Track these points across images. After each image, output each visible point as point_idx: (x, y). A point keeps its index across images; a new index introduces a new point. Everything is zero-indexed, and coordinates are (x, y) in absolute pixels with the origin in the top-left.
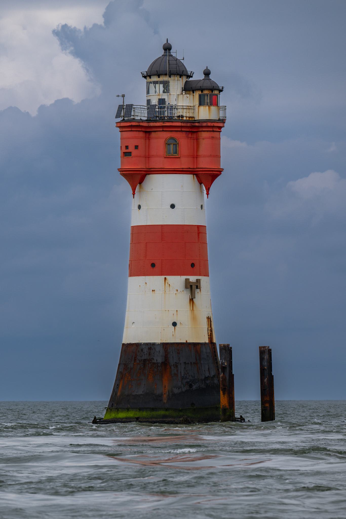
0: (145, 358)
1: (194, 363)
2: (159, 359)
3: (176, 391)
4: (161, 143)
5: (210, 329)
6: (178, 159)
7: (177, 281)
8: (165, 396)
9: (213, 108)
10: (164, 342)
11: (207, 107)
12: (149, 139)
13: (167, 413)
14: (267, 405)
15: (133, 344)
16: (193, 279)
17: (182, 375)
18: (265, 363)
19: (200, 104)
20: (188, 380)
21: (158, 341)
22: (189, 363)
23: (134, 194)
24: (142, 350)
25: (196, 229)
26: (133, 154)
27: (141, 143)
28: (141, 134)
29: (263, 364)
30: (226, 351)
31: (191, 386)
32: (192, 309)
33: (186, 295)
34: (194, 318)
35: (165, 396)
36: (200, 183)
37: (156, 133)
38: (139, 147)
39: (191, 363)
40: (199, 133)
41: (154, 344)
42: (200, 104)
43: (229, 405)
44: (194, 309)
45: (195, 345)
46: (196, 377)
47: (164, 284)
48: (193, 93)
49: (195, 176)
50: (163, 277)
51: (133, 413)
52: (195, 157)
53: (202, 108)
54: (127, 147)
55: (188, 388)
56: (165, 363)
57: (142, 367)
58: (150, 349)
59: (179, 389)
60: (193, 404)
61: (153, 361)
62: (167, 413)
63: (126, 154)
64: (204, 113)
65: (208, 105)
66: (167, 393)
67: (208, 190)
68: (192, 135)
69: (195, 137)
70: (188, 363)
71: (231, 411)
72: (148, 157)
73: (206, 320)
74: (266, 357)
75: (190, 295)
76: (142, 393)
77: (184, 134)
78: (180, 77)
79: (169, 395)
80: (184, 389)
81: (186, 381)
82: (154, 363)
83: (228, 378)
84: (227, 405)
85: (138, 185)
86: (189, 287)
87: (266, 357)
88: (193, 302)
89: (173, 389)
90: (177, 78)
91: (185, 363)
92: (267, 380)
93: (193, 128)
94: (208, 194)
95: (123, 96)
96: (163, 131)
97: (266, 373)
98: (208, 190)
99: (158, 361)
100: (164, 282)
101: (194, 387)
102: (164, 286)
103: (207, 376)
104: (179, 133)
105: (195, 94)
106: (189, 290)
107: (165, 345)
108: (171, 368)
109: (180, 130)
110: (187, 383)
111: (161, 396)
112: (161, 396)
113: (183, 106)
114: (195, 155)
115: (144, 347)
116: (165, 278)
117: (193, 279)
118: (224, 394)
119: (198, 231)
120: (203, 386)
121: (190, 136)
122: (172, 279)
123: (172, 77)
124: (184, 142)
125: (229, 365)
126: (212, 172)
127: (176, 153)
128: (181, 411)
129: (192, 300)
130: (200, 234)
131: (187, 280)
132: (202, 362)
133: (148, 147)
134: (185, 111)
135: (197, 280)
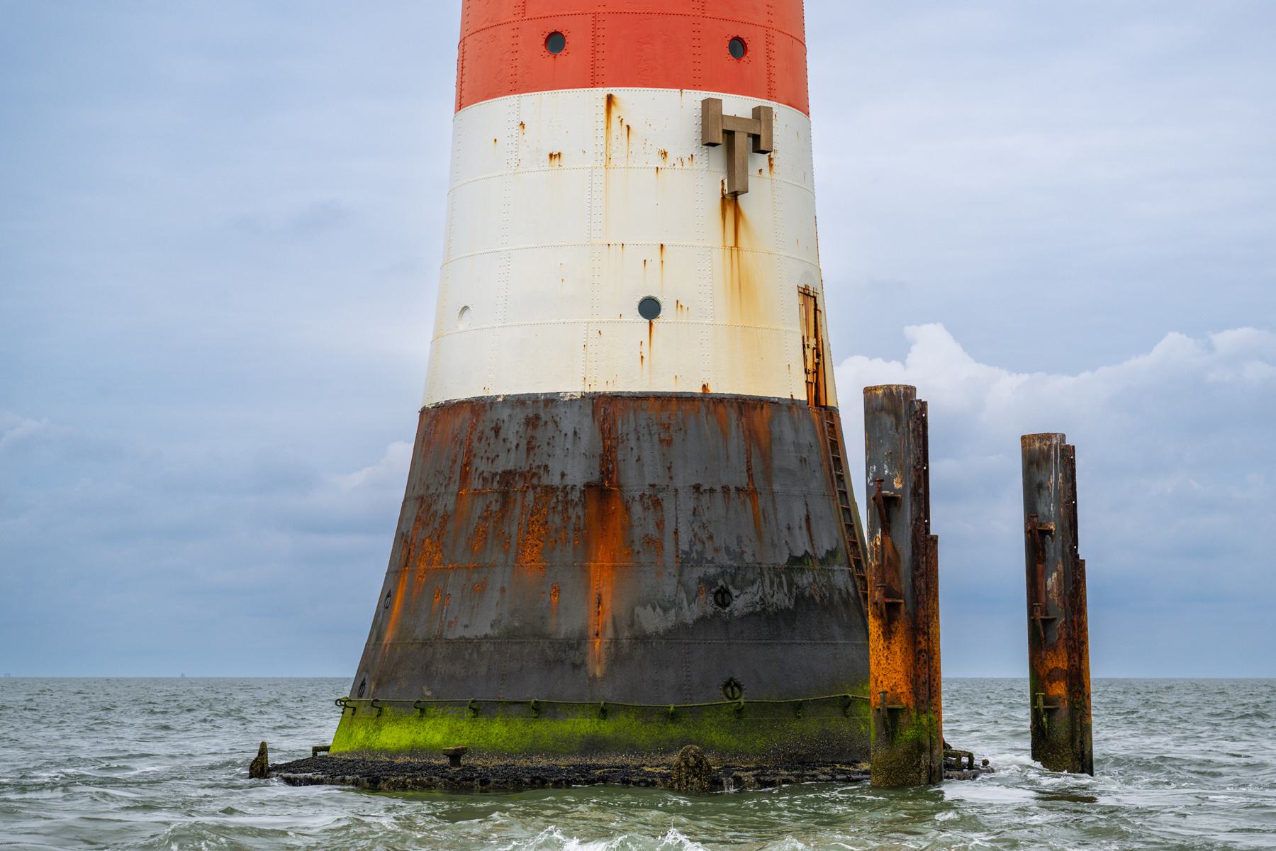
0: (510, 467)
1: (738, 489)
2: (572, 467)
3: (653, 621)
5: (812, 342)
8: (598, 647)
10: (602, 388)
13: (606, 728)
14: (1059, 689)
15: (460, 405)
16: (737, 106)
17: (684, 546)
18: (1049, 509)
20: (712, 571)
21: (571, 385)
22: (718, 488)
24: (497, 430)
30: (898, 418)
31: (723, 598)
32: (731, 242)
33: (707, 178)
34: (741, 286)
35: (598, 647)
39: (726, 490)
41: (551, 400)
43: (915, 692)
44: (743, 242)
45: (746, 405)
46: (748, 558)
47: (603, 126)
50: (601, 93)
51: (445, 729)
55: (710, 610)
56: (603, 490)
57: (495, 507)
58: (532, 422)
59: (665, 610)
60: (732, 685)
61: (545, 480)
62: (606, 728)
66: (609, 633)
70: (712, 490)
71: (924, 721)
73: (797, 300)
74: (1053, 479)
76: (488, 631)
79: (616, 641)
80: (691, 613)
81: (698, 572)
82: (549, 490)
83: (906, 552)
84: (903, 688)
86: (719, 138)
87: (1053, 479)
88: (737, 214)
89: (638, 610)
91: (697, 488)
92: (1058, 579)
97: (1053, 548)
99: (569, 481)
100: (603, 117)
102: (602, 133)
103: (799, 553)
106: (718, 154)
107: (606, 408)
108: (628, 510)
110: (707, 582)
111: (578, 643)
112: (578, 643)
115: (505, 414)
116: (610, 99)
117: (737, 106)
118: (888, 634)
120: (781, 599)
125: (915, 493)
128: (673, 717)
129: (731, 200)
132: (777, 487)
135: (757, 111)
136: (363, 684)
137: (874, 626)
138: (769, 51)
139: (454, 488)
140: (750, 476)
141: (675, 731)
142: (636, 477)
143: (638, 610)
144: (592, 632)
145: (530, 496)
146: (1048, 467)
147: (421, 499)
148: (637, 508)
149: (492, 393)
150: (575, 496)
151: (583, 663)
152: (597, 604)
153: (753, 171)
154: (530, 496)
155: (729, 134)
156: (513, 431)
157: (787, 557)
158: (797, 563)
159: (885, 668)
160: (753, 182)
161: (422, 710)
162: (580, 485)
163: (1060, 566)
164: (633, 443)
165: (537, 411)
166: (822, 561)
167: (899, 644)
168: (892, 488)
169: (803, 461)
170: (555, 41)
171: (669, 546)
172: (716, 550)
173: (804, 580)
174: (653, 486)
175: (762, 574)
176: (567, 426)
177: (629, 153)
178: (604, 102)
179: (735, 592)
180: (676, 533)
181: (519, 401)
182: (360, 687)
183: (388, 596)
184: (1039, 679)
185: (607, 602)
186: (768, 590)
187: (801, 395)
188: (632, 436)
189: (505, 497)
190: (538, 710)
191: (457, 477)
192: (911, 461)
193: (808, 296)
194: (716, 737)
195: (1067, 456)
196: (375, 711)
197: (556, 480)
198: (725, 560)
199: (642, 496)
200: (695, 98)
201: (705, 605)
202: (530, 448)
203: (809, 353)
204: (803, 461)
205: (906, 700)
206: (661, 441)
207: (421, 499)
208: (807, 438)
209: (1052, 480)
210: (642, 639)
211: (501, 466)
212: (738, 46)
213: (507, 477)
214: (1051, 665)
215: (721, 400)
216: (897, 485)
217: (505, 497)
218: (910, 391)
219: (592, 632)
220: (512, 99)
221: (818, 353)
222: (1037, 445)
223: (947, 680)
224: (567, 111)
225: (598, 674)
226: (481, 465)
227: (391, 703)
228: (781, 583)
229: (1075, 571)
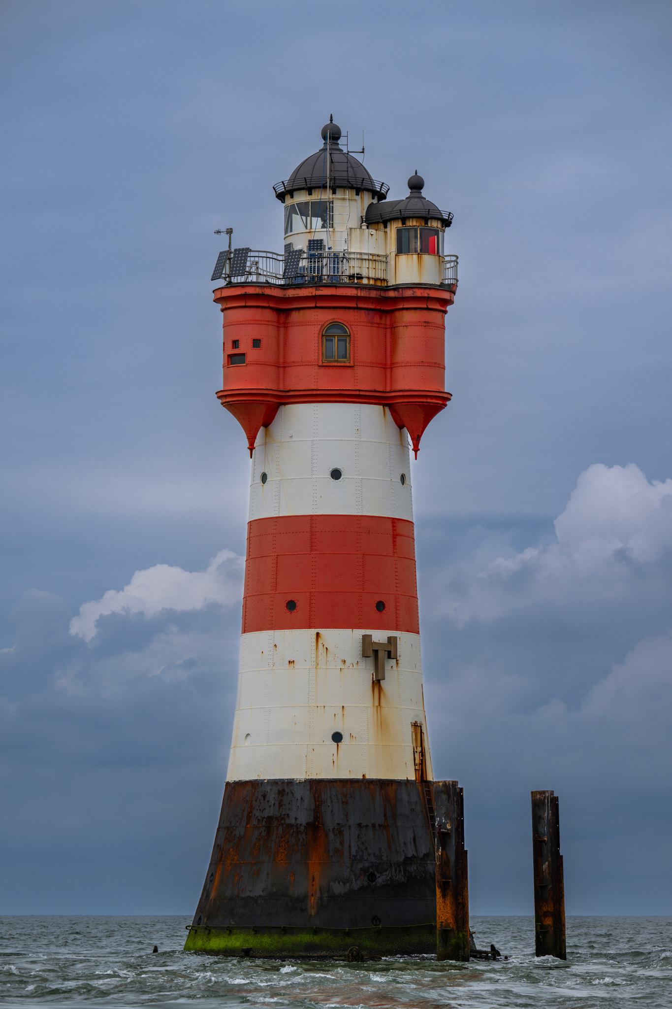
0: (271, 814)
1: (379, 825)
2: (301, 816)
3: (338, 889)
4: (313, 332)
5: (419, 749)
6: (349, 370)
7: (345, 641)
8: (313, 901)
9: (427, 259)
10: (314, 777)
11: (415, 257)
12: (286, 326)
13: (317, 939)
14: (549, 921)
15: (247, 782)
16: (379, 636)
17: (353, 853)
18: (545, 829)
19: (400, 251)
20: (367, 865)
21: (300, 775)
22: (370, 825)
23: (251, 448)
24: (264, 796)
25: (389, 525)
26: (249, 358)
27: (267, 333)
28: (268, 315)
29: (541, 829)
30: (449, 796)
31: (372, 877)
32: (377, 704)
33: (364, 674)
34: (382, 725)
35: (313, 901)
36: (401, 427)
37: (301, 312)
38: (264, 344)
39: (374, 825)
40: (397, 313)
41: (290, 782)
42: (400, 251)
43: (457, 922)
44: (383, 704)
45: (384, 784)
46: (384, 858)
47: (314, 648)
48: (386, 227)
49: (387, 409)
50: (314, 631)
51: (241, 940)
52: (387, 366)
53: (403, 258)
54: (235, 344)
55: (366, 883)
56: (315, 826)
57: (264, 834)
58: (281, 793)
59: (344, 884)
60: (376, 919)
61: (288, 821)
62: (317, 939)
63: (234, 359)
64: (408, 271)
65: (416, 251)
66: (318, 894)
67: (416, 440)
68: (381, 318)
69: (388, 322)
70: (367, 826)
71: (461, 935)
72: (281, 366)
73: (410, 730)
74: (547, 814)
75: (373, 671)
76: (261, 893)
78: (357, 194)
79: (321, 899)
80: (356, 885)
81: (360, 866)
82: (290, 826)
83: (452, 858)
84: (451, 920)
86: (371, 653)
87: (547, 814)
88: (380, 690)
89: (332, 883)
90: (348, 194)
91: (360, 825)
92: (549, 866)
93: (384, 303)
94: (416, 449)
95: (230, 232)
96: (316, 307)
97: (546, 850)
98: (416, 440)
99: (299, 822)
100: (314, 644)
101: (380, 880)
102: (314, 652)
103: (410, 856)
104: (351, 312)
105: (388, 230)
106: (371, 661)
107: (315, 785)
108: (327, 836)
109: (353, 305)
110: (364, 870)
111: (303, 899)
112: (303, 899)
113: (361, 254)
114: (389, 362)
115: (268, 788)
116: (318, 634)
117: (379, 636)
118: (444, 896)
119: (394, 530)
120: (400, 878)
121: (377, 319)
122: (330, 635)
123: (339, 194)
124: (362, 332)
125: (457, 830)
126: (425, 400)
127: (345, 357)
128: (348, 934)
129: (377, 684)
130: (399, 539)
131: (366, 638)
132: (399, 824)
133: (283, 344)
134: (365, 264)
135: (389, 638)
136: (200, 919)
137: (438, 892)
138: (397, 606)
139: (244, 824)
140: (386, 819)
141: (349, 940)
142: (330, 822)
143: (332, 883)
144: (310, 894)
145: (281, 829)
146: (545, 809)
147: (228, 828)
148: (331, 835)
149: (262, 778)
150: (302, 829)
151: (306, 909)
152: (312, 880)
153: (387, 668)
154: (281, 829)
155: (376, 652)
156: (272, 797)
157: (403, 857)
158: (409, 860)
159: (443, 911)
160: (388, 674)
161: (230, 931)
162: (304, 823)
163: (550, 859)
164: (329, 804)
165: (284, 787)
166: (421, 859)
167: (449, 901)
168: (446, 828)
169: (413, 810)
170: (291, 605)
171: (346, 852)
172: (369, 855)
173: (412, 869)
174: (339, 824)
175: (391, 866)
176: (298, 795)
177: (327, 661)
178: (315, 636)
179: (378, 875)
180: (350, 846)
181: (275, 783)
182: (198, 920)
183: (211, 876)
184: (539, 917)
185: (317, 880)
186: (394, 874)
187: (412, 777)
188: (329, 800)
189: (269, 830)
190: (285, 931)
191: (245, 818)
192: (455, 815)
193: (417, 727)
194: (368, 943)
195: (554, 802)
196: (207, 932)
197: (293, 821)
198: (373, 860)
199: (333, 829)
200: (359, 633)
201: (363, 881)
202: (280, 806)
203: (417, 756)
204: (413, 810)
205: (452, 926)
206: (343, 802)
207: (228, 828)
208: (415, 798)
209: (546, 815)
210: (333, 897)
211: (266, 814)
212: (380, 606)
213: (269, 819)
214: (544, 909)
215: (372, 782)
216: (449, 827)
217: (269, 830)
218: (455, 784)
219: (310, 894)
220: (271, 632)
221: (423, 753)
222: (538, 796)
223: (474, 917)
224: (297, 640)
225: (313, 913)
226: (257, 813)
227: (215, 928)
228: (400, 871)
229: (558, 862)
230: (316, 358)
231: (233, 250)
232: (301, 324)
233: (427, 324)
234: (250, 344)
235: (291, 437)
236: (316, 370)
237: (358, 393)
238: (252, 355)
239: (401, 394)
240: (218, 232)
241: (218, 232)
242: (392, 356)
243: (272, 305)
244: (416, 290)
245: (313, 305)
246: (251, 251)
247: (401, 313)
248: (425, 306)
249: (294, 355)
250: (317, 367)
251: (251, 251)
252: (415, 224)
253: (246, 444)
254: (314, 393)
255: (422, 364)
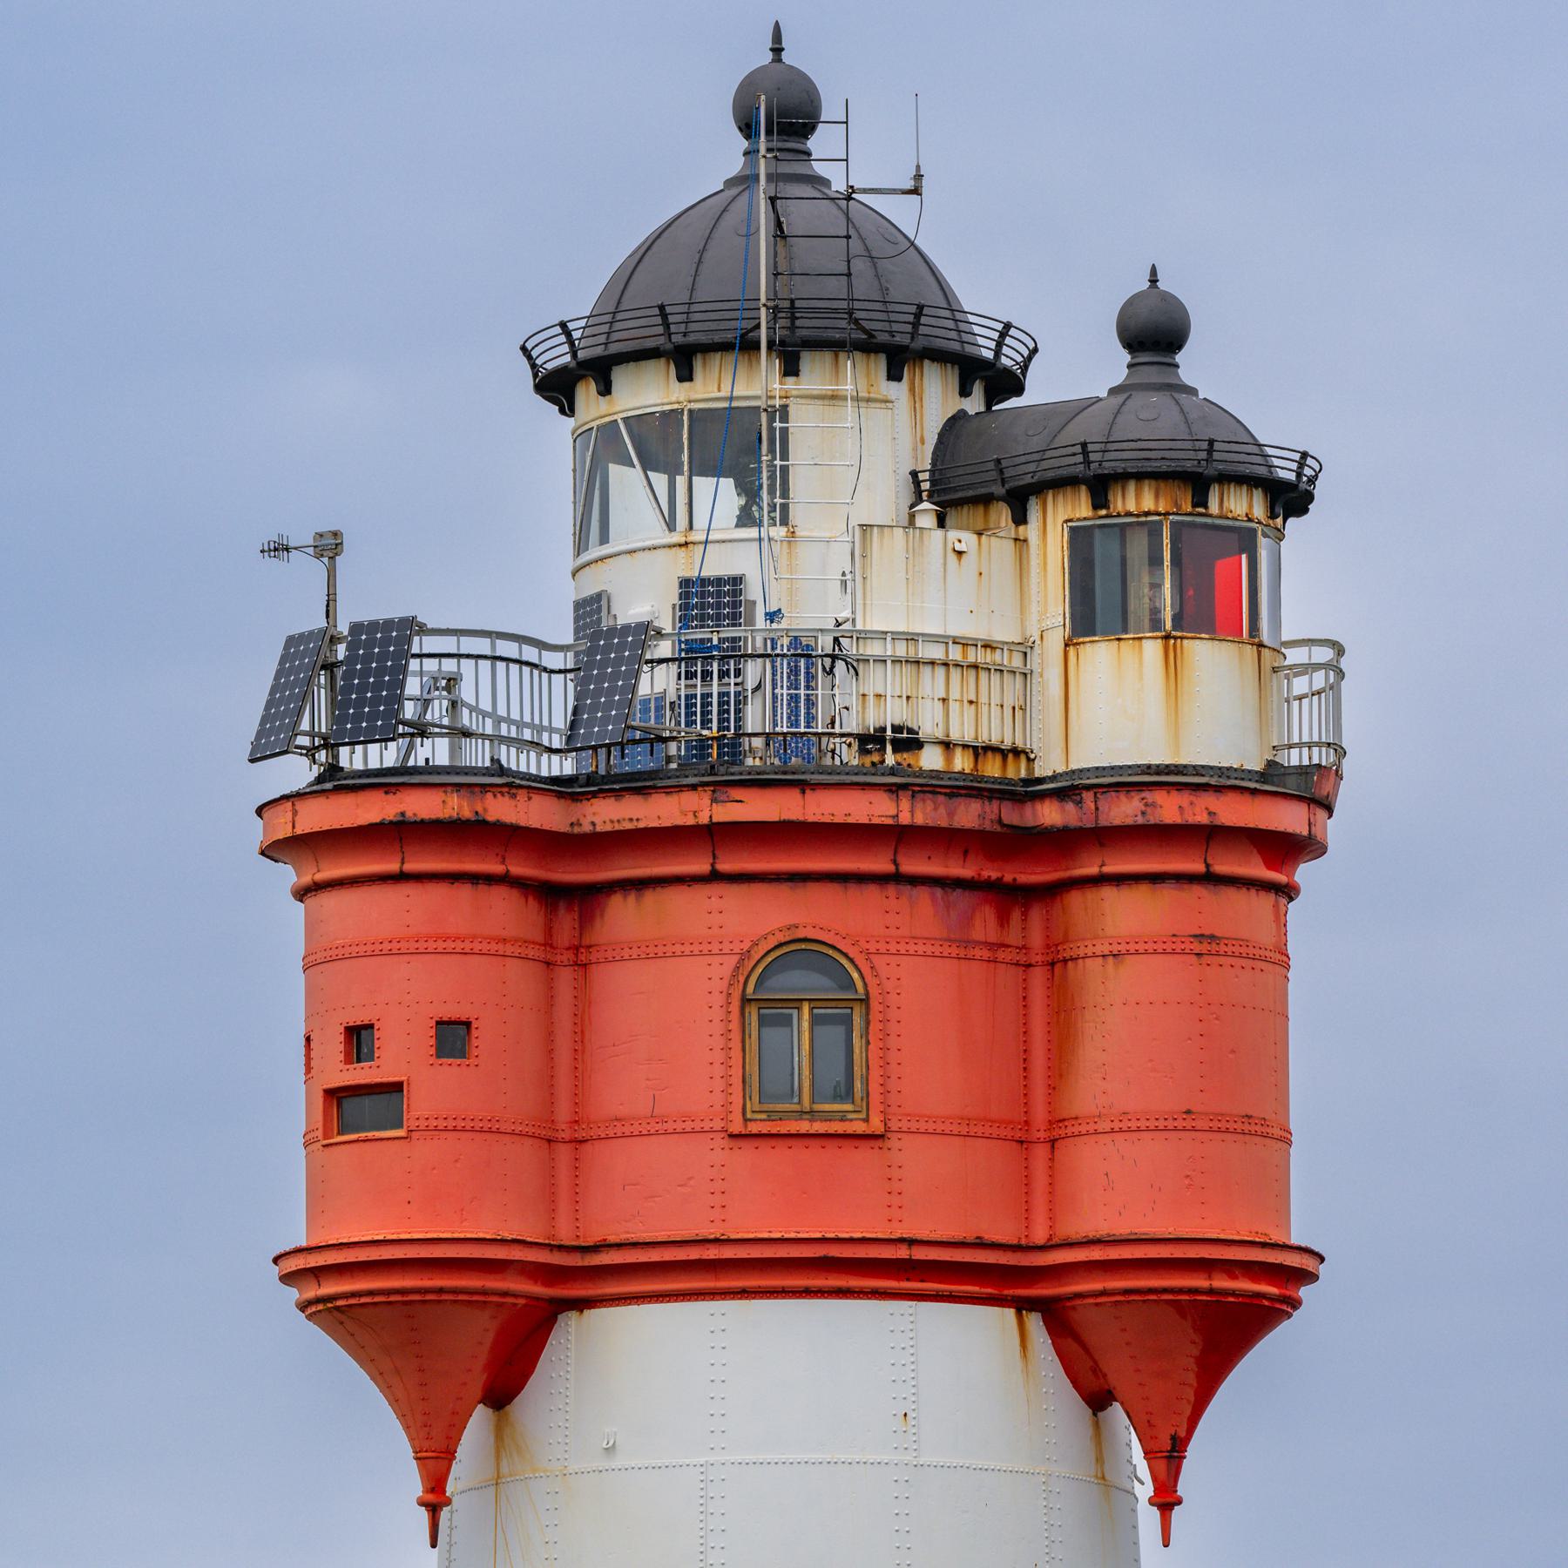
6: (863, 1155)
12: (582, 959)
23: (435, 1502)
27: (496, 992)
28: (505, 913)
36: (1097, 1400)
37: (651, 897)
38: (483, 1038)
40: (1075, 899)
48: (1020, 519)
49: (1035, 1322)
53: (1099, 656)
64: (1122, 710)
67: (1168, 1457)
68: (1003, 920)
69: (1036, 939)
77: (920, 914)
85: (481, 1416)
94: (1166, 1501)
95: (329, 547)
96: (715, 877)
105: (1031, 531)
109: (879, 863)
114: (1040, 1114)
121: (984, 925)
126: (1200, 1282)
127: (847, 1094)
134: (932, 683)
230: (718, 1098)
231: (343, 628)
232: (653, 952)
233: (1206, 945)
234: (426, 1038)
235: (610, 1450)
236: (716, 1152)
237: (902, 1253)
238: (434, 1088)
239: (1096, 1254)
240: (279, 549)
241: (279, 549)
242: (1052, 1088)
243: (517, 869)
244: (1158, 797)
245: (701, 866)
246: (423, 630)
247: (1092, 896)
248: (1198, 867)
249: (622, 1089)
250: (720, 1141)
251: (423, 630)
252: (1148, 503)
253: (415, 1486)
254: (712, 1253)
255: (1184, 1122)
